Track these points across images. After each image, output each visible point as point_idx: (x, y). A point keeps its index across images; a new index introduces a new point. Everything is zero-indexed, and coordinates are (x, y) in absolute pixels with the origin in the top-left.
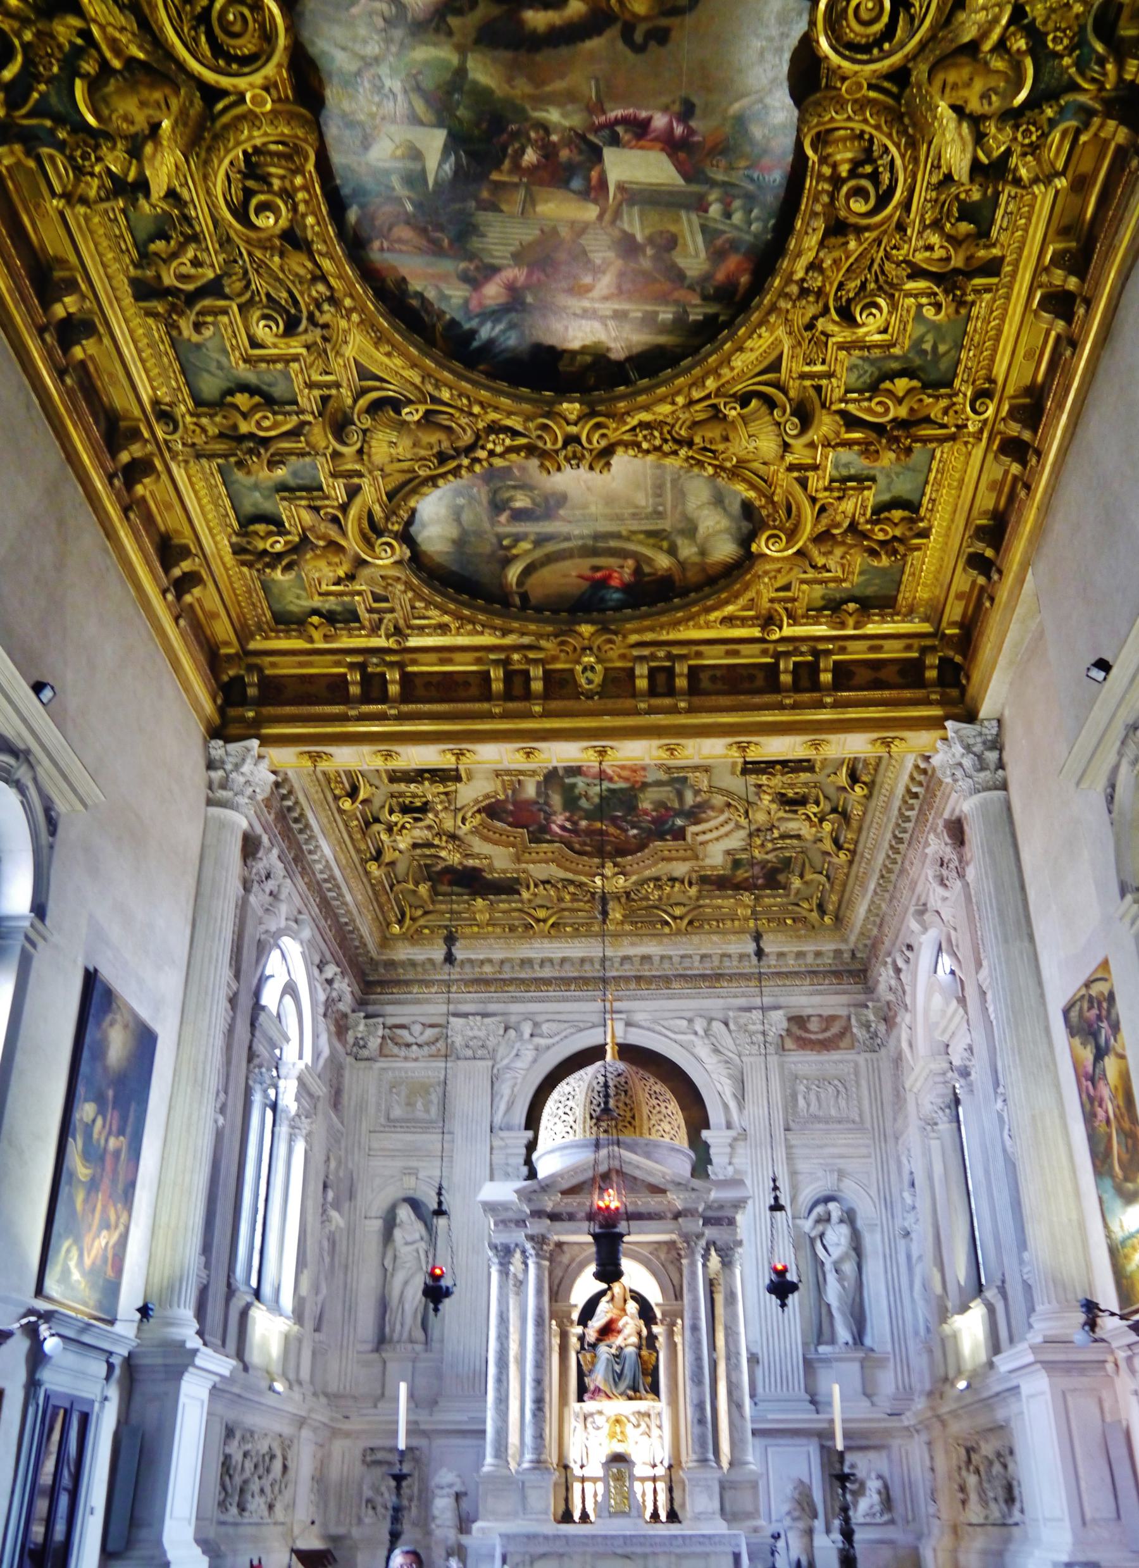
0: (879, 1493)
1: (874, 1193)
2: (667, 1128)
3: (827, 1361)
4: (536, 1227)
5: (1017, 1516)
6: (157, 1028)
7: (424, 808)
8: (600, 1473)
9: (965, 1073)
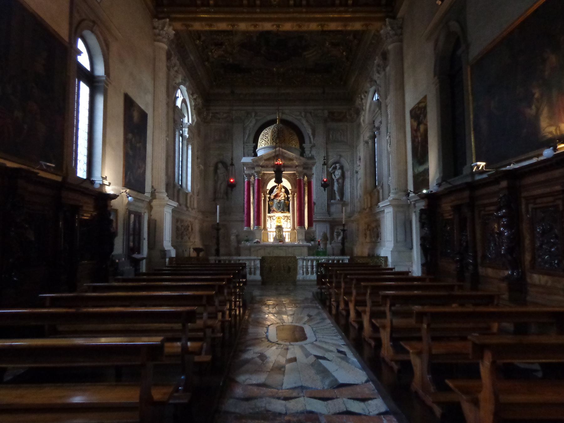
2: (294, 143)
3: (333, 204)
4: (257, 169)
5: (379, 240)
6: (147, 112)
7: (221, 44)
8: (274, 230)
9: (378, 129)
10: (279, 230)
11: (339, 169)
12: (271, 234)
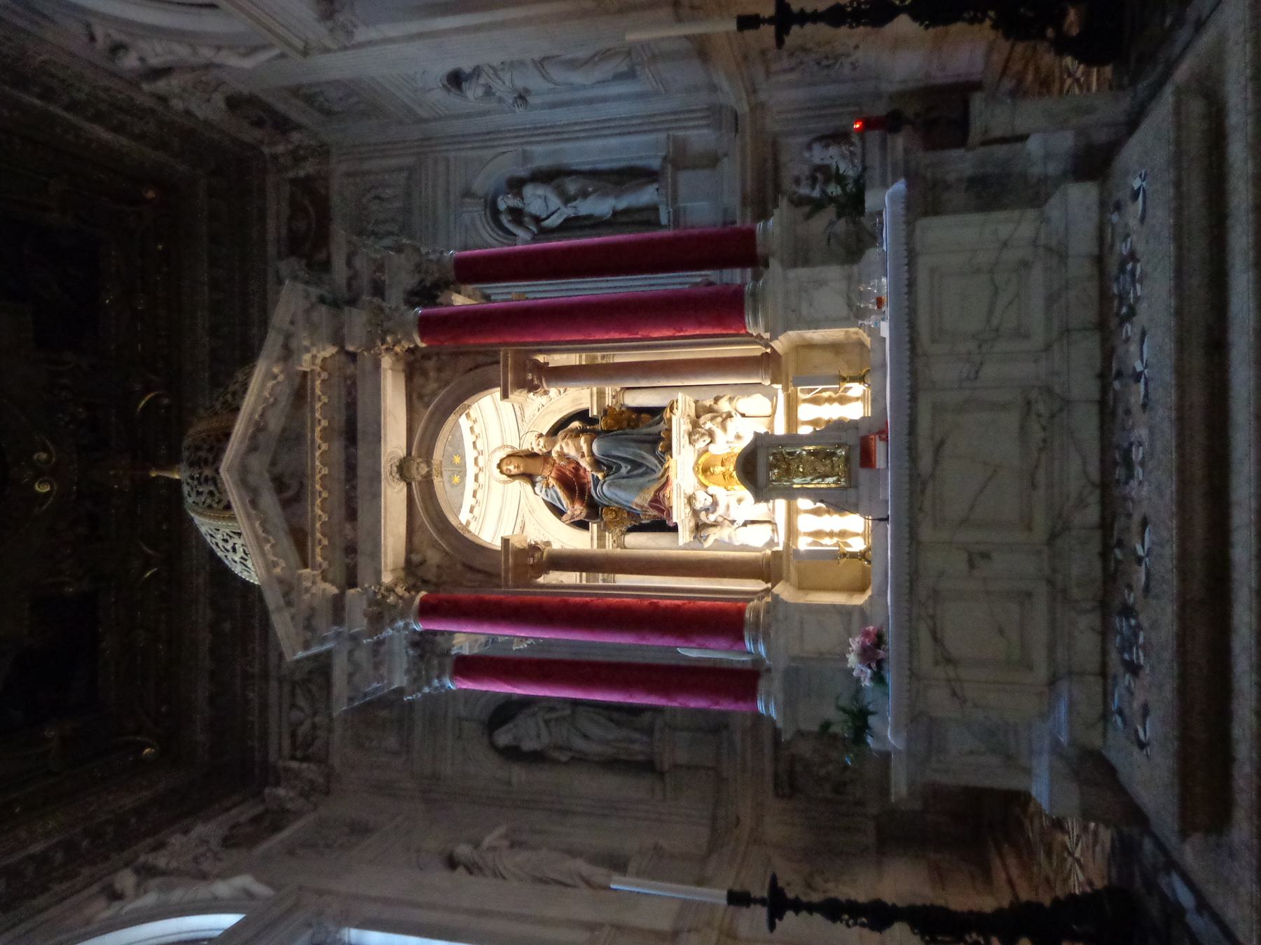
0: (827, 146)
1: (488, 153)
8: (781, 504)
10: (771, 466)
11: (519, 194)
12: (806, 523)
